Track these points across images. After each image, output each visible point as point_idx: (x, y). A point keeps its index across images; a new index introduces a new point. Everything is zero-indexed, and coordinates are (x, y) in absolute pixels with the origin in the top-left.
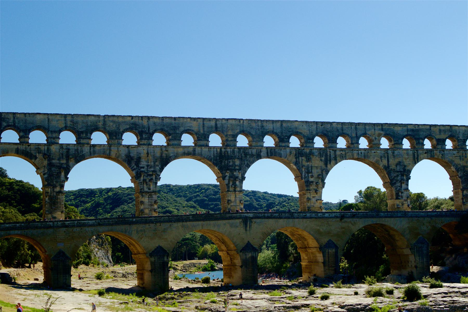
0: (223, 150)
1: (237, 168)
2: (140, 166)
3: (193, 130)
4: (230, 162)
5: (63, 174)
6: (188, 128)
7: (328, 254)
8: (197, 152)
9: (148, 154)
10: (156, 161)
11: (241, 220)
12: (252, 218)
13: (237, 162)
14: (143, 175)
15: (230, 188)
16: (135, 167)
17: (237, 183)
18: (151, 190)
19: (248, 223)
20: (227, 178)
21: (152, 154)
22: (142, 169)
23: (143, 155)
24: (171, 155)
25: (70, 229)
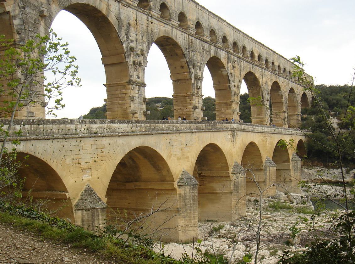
5: (42, 24)
7: (270, 172)
13: (199, 56)
14: (132, 54)
16: (125, 38)
20: (193, 75)
24: (155, 31)
25: (100, 141)
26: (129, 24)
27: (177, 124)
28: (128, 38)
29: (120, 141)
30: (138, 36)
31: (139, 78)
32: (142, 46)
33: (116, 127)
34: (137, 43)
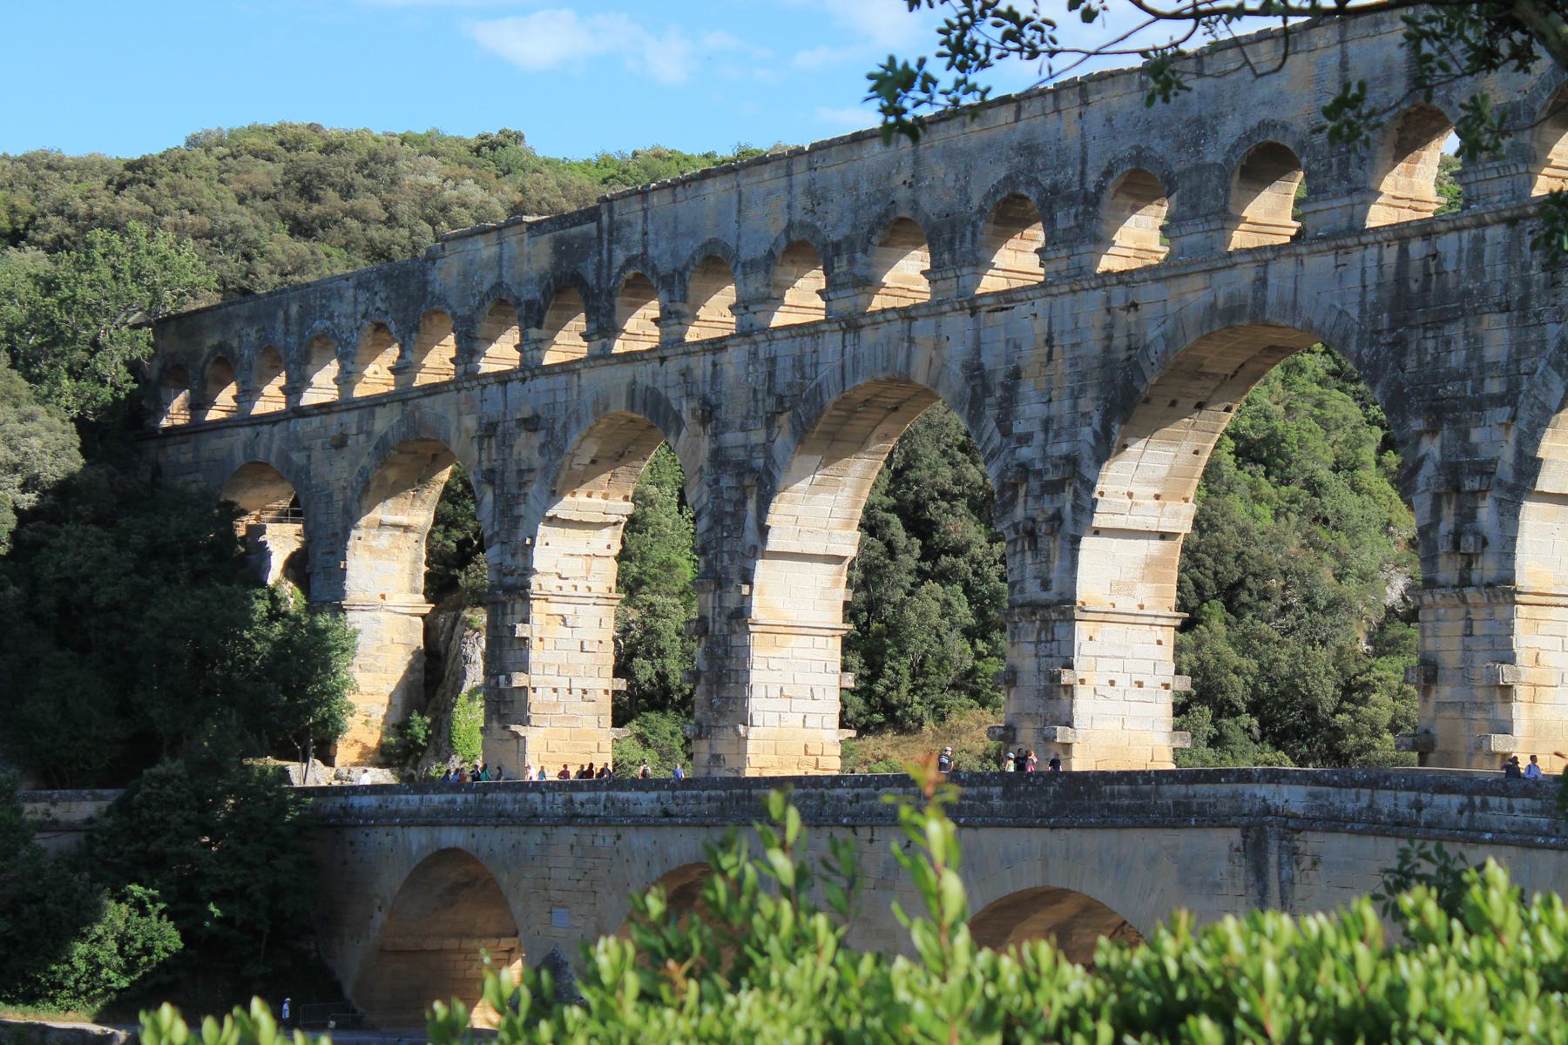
0: (1417, 248)
1: (1494, 386)
2: (1019, 428)
3: (1285, 127)
4: (1448, 343)
6: (1264, 114)
8: (1272, 295)
9: (1049, 341)
10: (1082, 390)
11: (1235, 835)
12: (1307, 823)
13: (1497, 338)
15: (1442, 561)
16: (997, 439)
17: (1486, 513)
18: (1055, 587)
19: (1273, 859)
21: (1068, 341)
22: (1025, 453)
23: (1031, 355)
26: (1016, 374)
27: (839, 791)
28: (1006, 432)
29: (639, 840)
30: (1055, 404)
31: (1046, 585)
32: (1073, 437)
33: (628, 801)
34: (1051, 435)
